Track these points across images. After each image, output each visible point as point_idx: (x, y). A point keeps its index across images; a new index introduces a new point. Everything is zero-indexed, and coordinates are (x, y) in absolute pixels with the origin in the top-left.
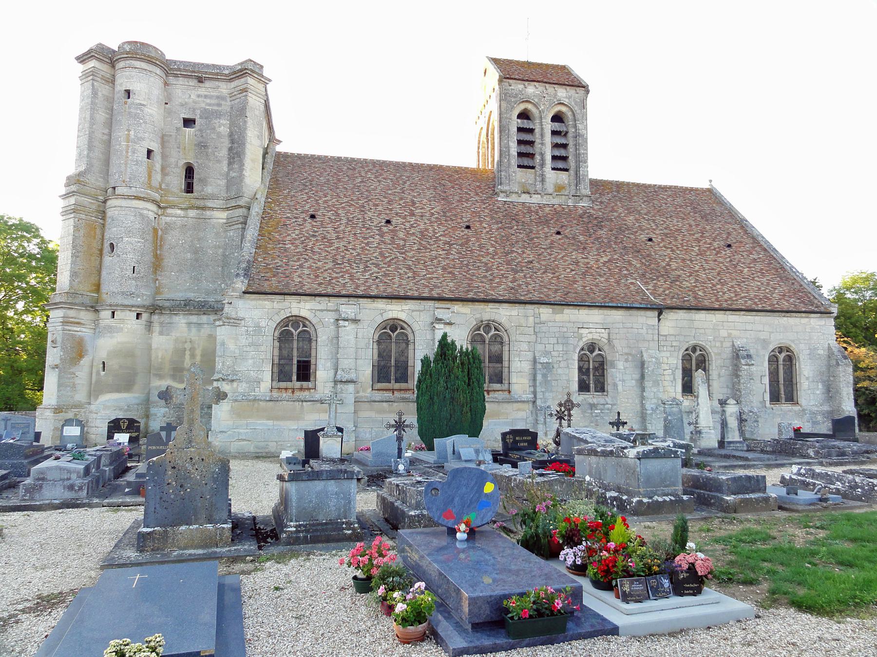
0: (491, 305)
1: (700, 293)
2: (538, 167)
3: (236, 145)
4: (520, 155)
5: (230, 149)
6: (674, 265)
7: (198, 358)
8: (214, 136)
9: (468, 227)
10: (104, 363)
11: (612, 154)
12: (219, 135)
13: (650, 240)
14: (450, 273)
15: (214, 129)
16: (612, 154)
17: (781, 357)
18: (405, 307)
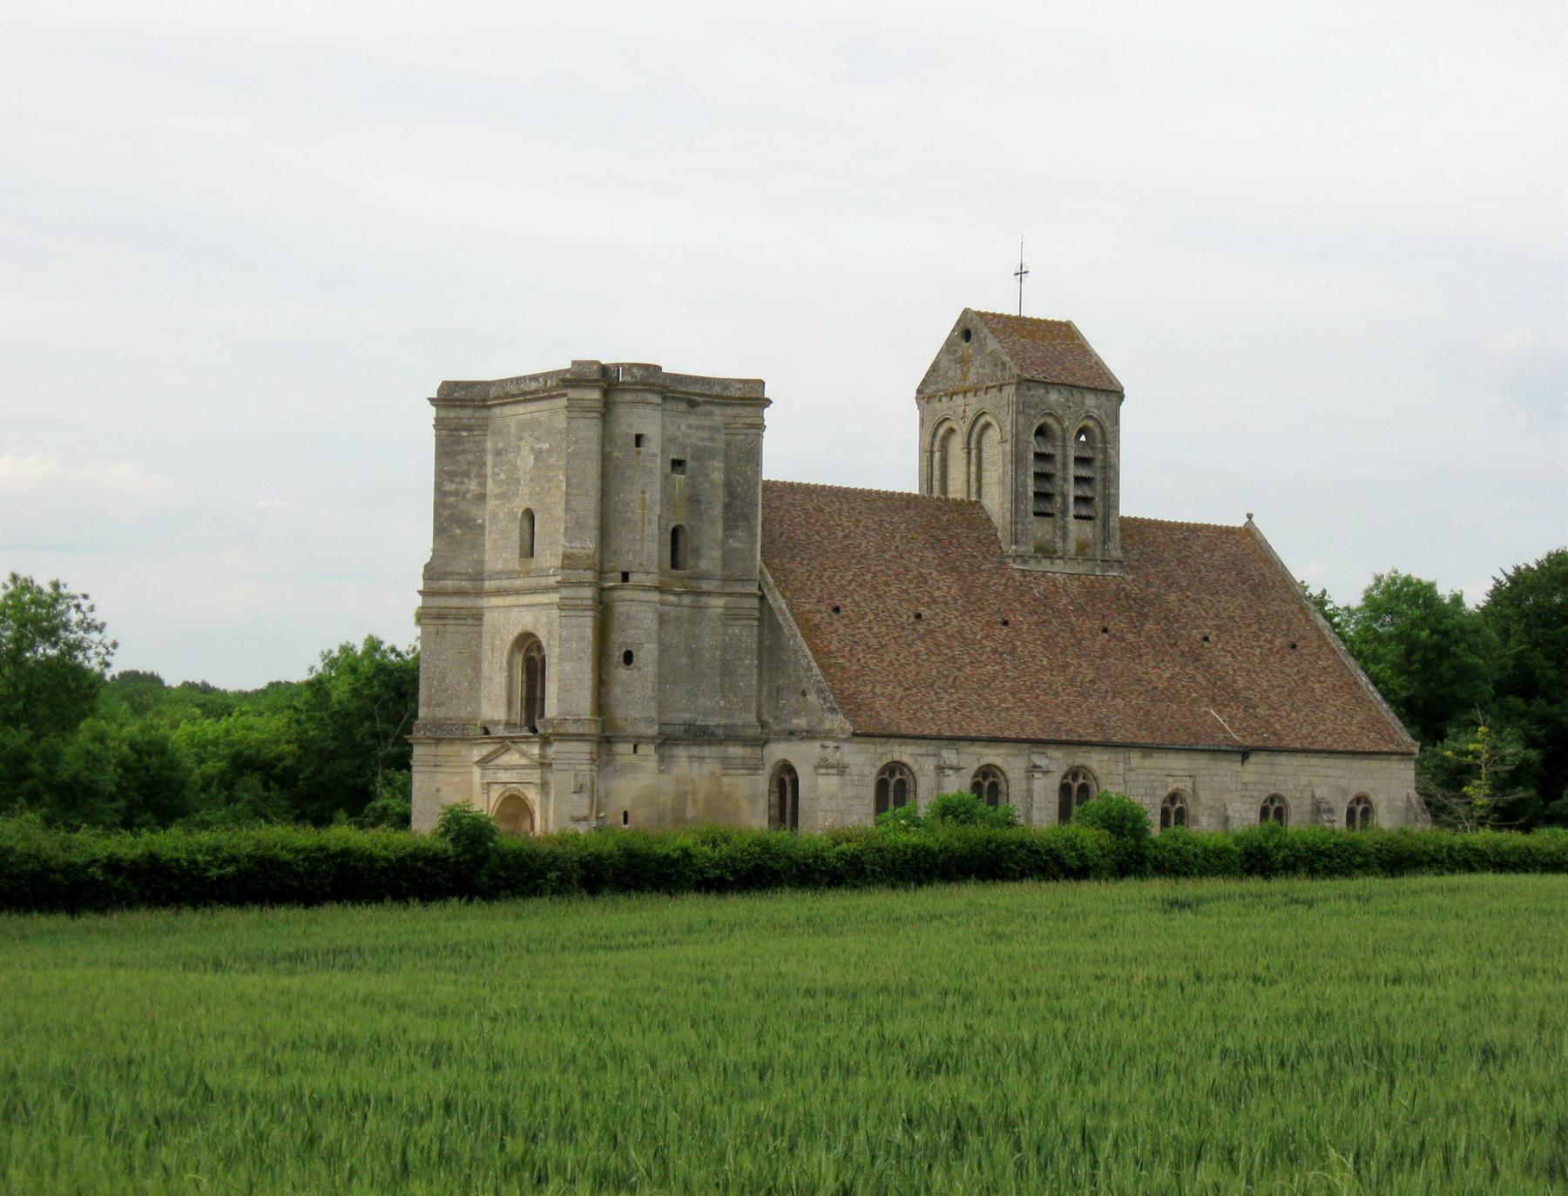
0: (1084, 748)
1: (1277, 726)
2: (1058, 515)
3: (738, 502)
4: (1037, 494)
5: (727, 506)
6: (1241, 683)
7: (701, 804)
8: (706, 485)
9: (1005, 623)
10: (626, 814)
11: (1148, 487)
12: (712, 483)
13: (1206, 639)
14: (1022, 700)
15: (706, 475)
16: (1148, 487)
17: (1360, 808)
18: (1002, 751)
